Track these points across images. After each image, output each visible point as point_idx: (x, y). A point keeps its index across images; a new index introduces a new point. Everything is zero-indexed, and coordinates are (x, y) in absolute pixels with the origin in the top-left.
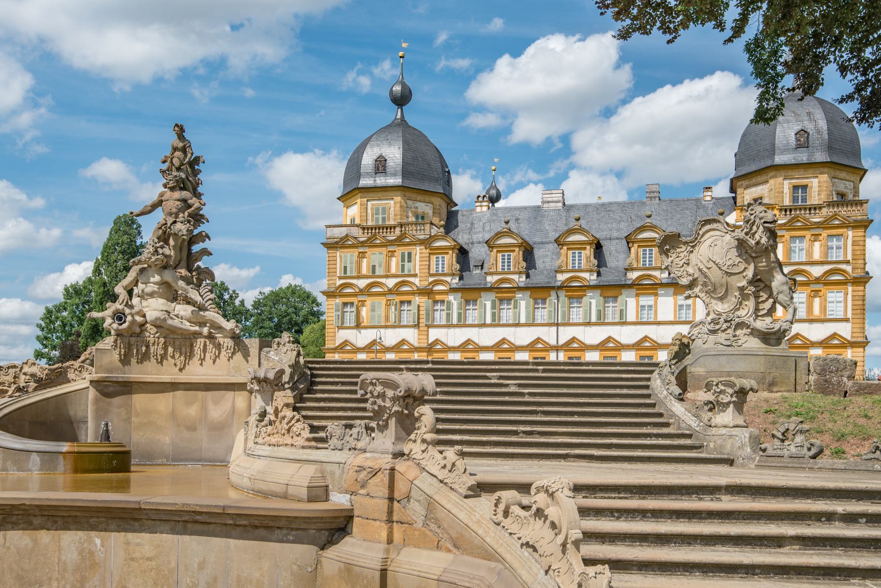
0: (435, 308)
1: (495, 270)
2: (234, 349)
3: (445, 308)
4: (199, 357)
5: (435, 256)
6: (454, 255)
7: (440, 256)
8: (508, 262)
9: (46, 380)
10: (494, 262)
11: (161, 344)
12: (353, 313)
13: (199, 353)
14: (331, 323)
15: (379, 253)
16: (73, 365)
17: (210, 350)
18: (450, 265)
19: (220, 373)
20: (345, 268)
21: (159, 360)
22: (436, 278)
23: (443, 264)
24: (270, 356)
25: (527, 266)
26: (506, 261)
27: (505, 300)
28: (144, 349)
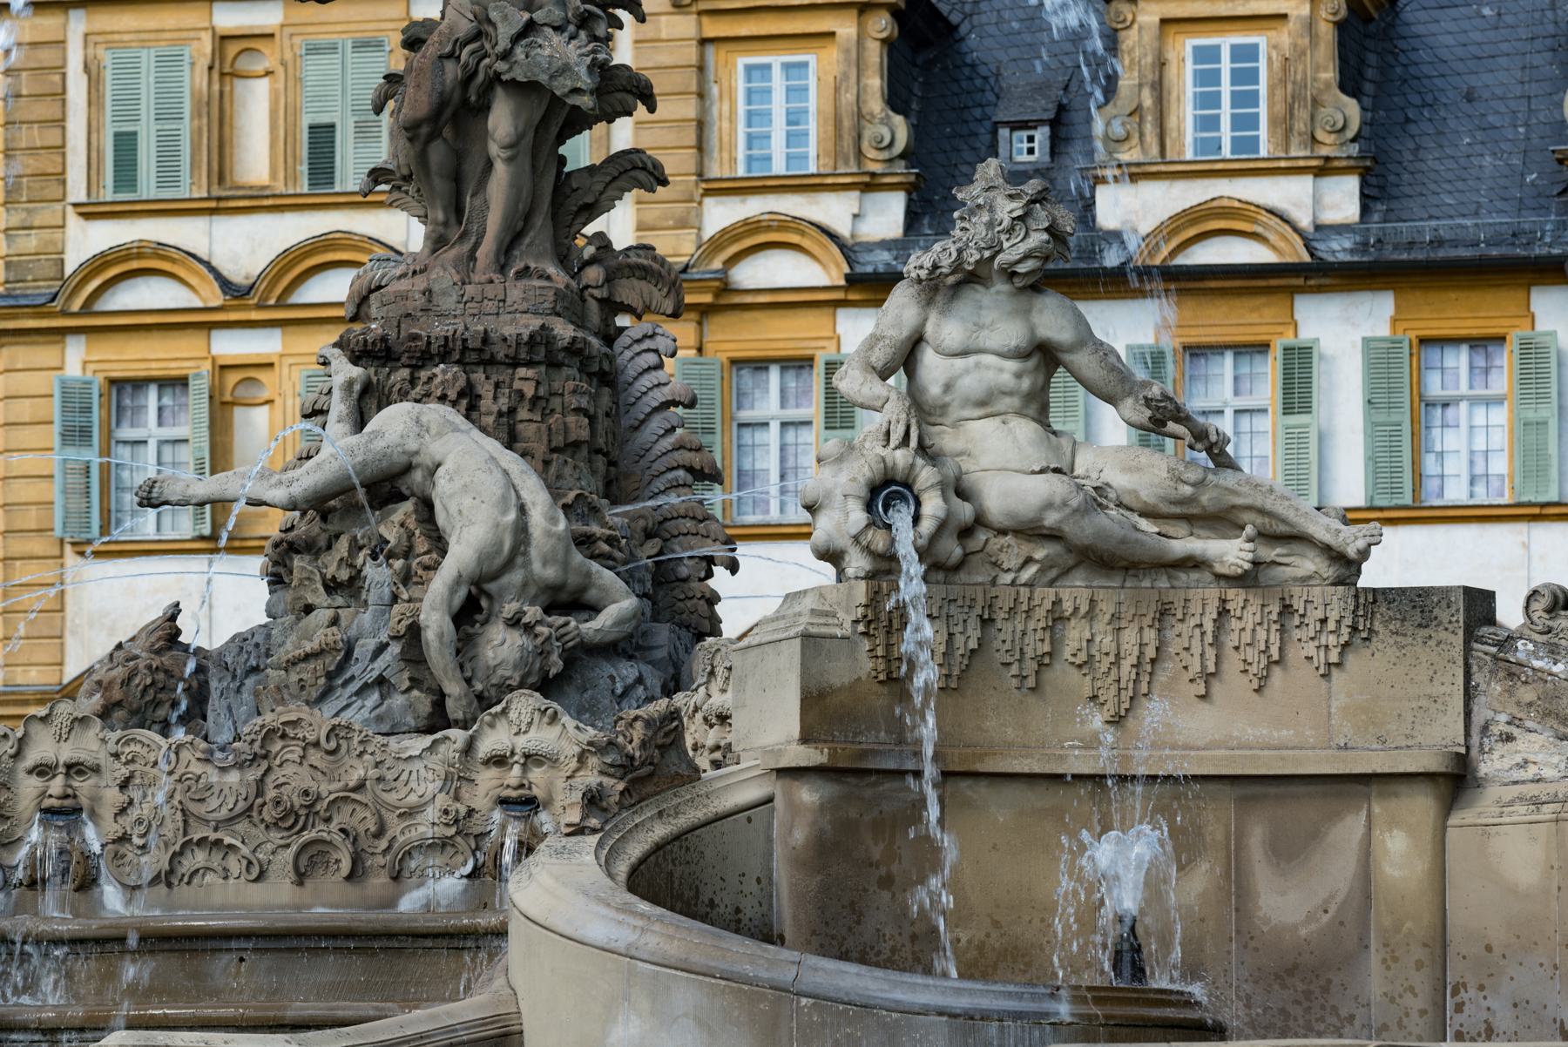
0: (746, 415)
1: (1154, 151)
2: (1354, 629)
3: (814, 409)
4: (1196, 667)
5: (742, 61)
6: (874, 54)
7: (776, 60)
8: (1238, 99)
9: (643, 764)
10: (1148, 100)
11: (1040, 613)
12: (185, 454)
13: (1196, 650)
14: (30, 519)
15: (361, 45)
16: (294, 724)
17: (1247, 638)
18: (847, 123)
19: (1286, 734)
20: (126, 144)
21: (1031, 682)
22: (754, 207)
23: (794, 118)
24: (1521, 656)
25: (1363, 123)
26: (1226, 88)
27: (1219, 348)
28: (974, 633)
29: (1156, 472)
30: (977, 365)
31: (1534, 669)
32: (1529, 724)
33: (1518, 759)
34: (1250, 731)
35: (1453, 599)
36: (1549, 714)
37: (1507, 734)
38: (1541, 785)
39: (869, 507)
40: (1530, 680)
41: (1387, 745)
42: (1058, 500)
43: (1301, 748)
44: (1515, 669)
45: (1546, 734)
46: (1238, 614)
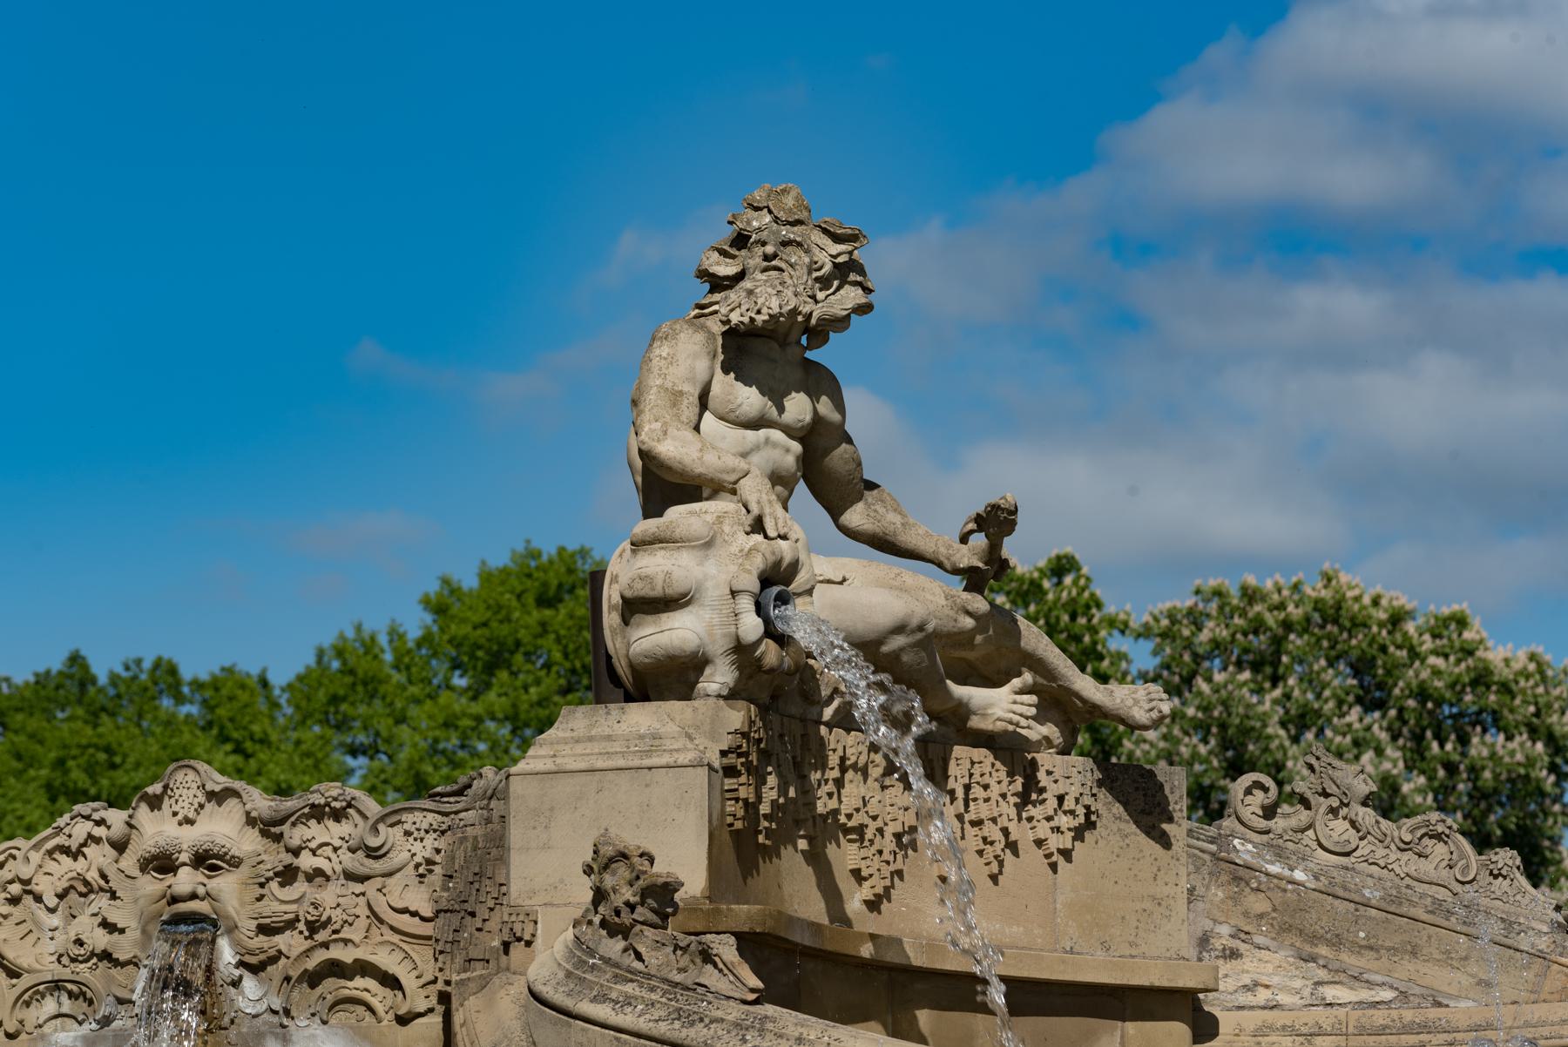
24: (1248, 858)
29: (929, 597)
30: (767, 441)
31: (1267, 874)
32: (1259, 939)
33: (1247, 980)
34: (985, 925)
35: (1176, 783)
36: (1289, 929)
37: (1231, 949)
38: (1275, 1013)
39: (760, 609)
40: (1263, 887)
41: (1110, 952)
42: (915, 622)
43: (1031, 949)
44: (1242, 872)
45: (1283, 953)
46: (986, 780)
